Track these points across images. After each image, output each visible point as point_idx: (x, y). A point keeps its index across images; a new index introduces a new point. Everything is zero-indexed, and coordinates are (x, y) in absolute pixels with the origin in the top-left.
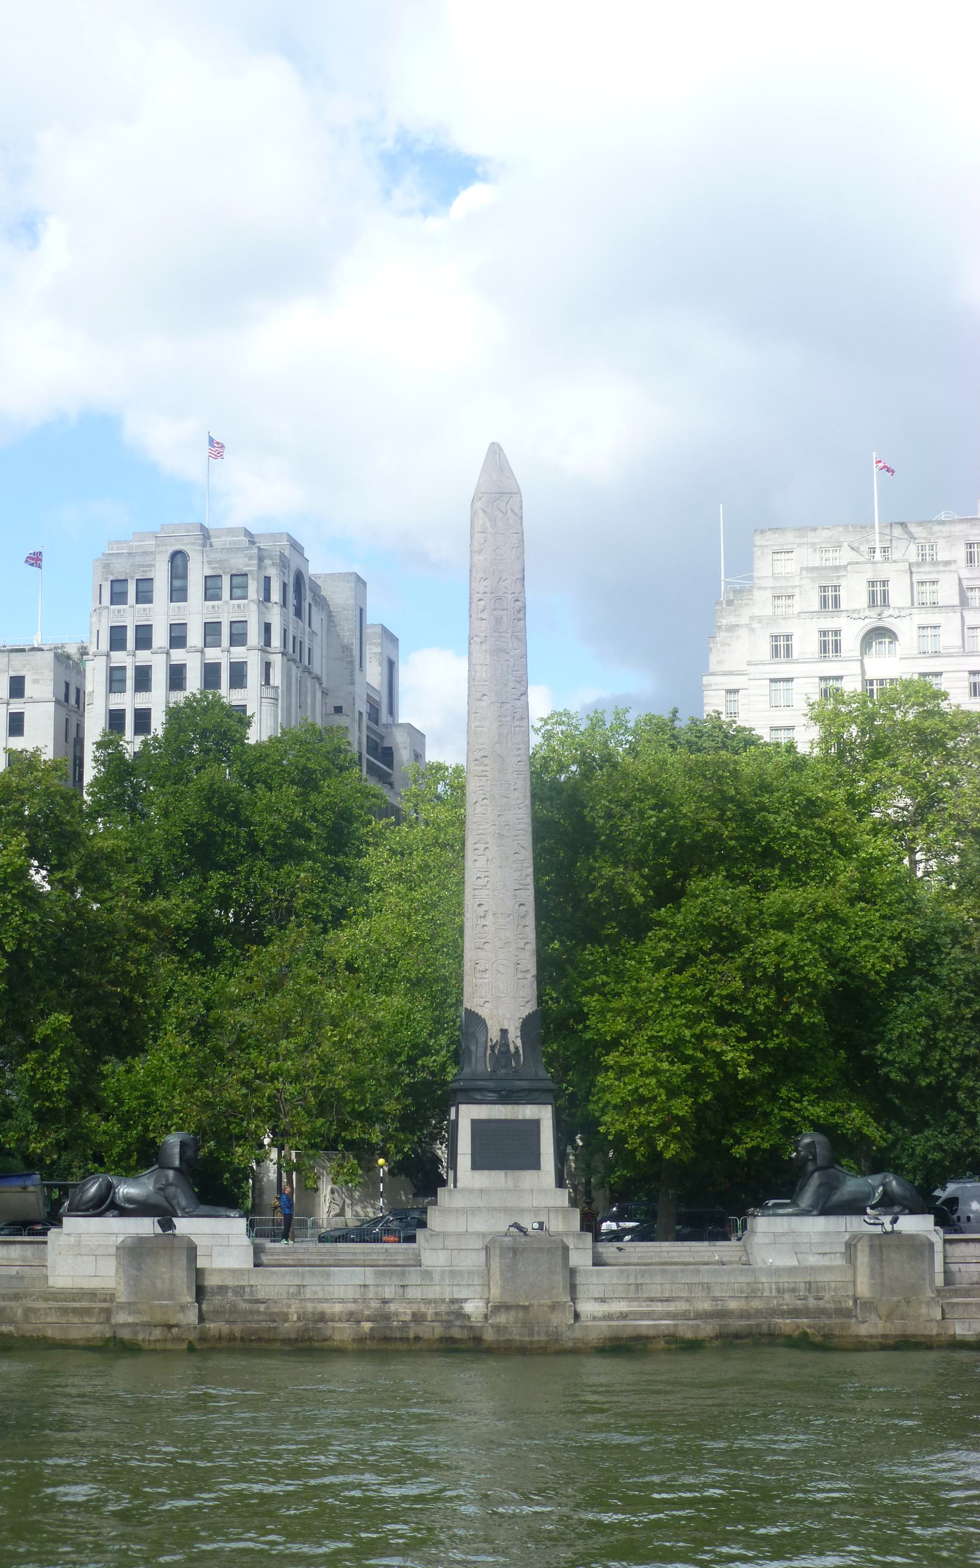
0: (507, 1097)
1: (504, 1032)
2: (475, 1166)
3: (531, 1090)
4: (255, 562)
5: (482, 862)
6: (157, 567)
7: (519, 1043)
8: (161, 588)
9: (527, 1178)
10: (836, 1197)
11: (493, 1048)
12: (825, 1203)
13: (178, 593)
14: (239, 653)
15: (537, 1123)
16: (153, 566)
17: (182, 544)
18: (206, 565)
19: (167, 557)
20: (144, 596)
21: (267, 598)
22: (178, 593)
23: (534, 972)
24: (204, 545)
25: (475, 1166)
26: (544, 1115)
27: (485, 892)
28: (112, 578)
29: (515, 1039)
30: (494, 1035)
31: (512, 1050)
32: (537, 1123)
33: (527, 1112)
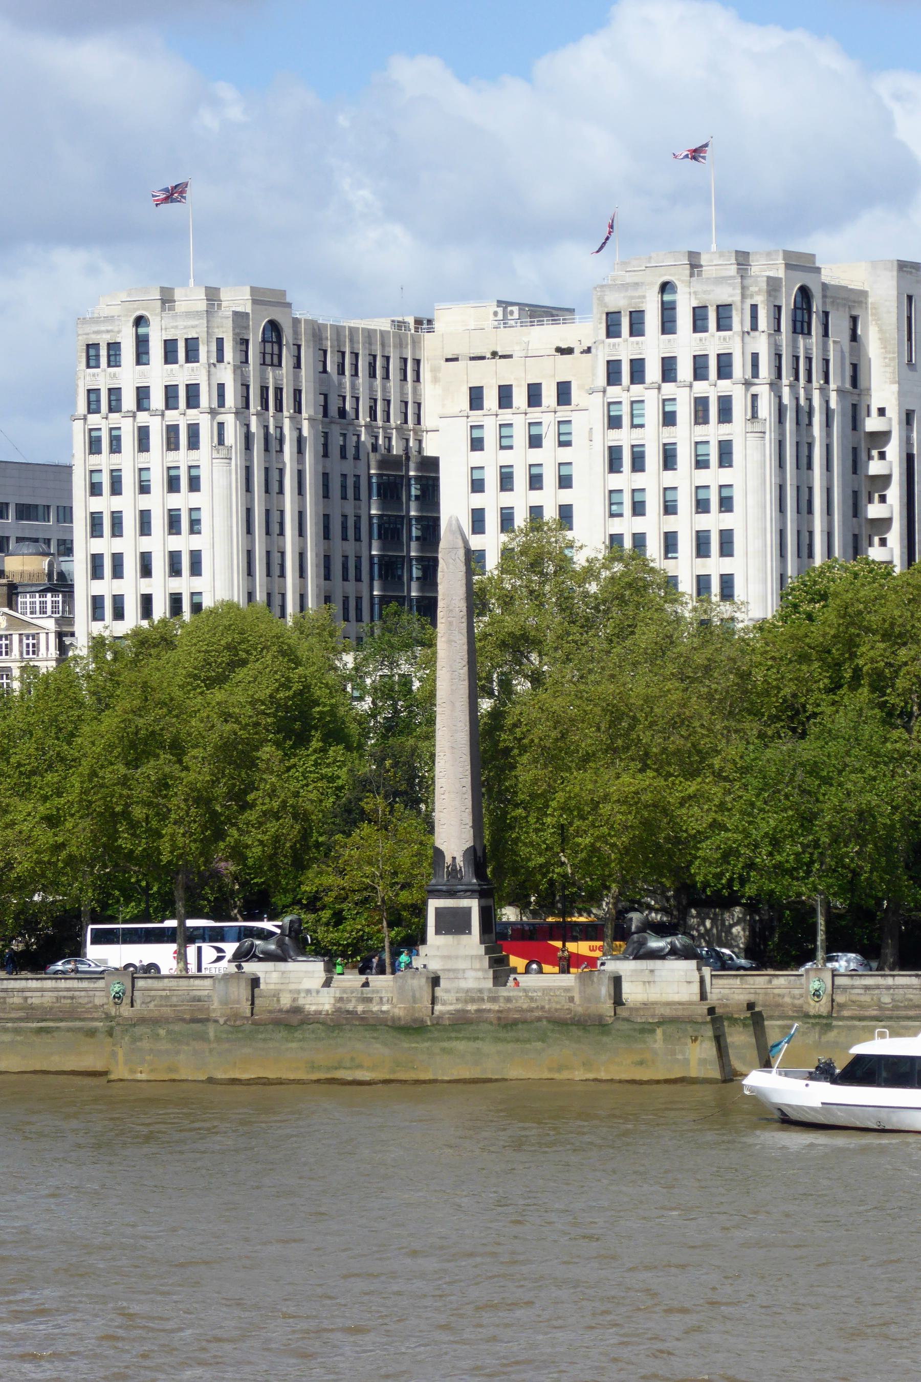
0: (451, 894)
1: (454, 858)
2: (438, 932)
3: (466, 891)
4: (739, 291)
5: (442, 762)
6: (648, 299)
7: (462, 864)
8: (652, 320)
9: (464, 938)
10: (642, 951)
11: (448, 867)
12: (638, 952)
13: (668, 325)
14: (725, 386)
15: (470, 908)
16: (644, 297)
17: (671, 275)
18: (693, 296)
19: (657, 288)
20: (637, 329)
21: (754, 327)
22: (668, 325)
23: (471, 824)
24: (692, 275)
25: (438, 932)
26: (473, 904)
27: (444, 780)
28: (606, 310)
29: (460, 862)
30: (448, 860)
31: (458, 868)
32: (470, 908)
33: (464, 903)
